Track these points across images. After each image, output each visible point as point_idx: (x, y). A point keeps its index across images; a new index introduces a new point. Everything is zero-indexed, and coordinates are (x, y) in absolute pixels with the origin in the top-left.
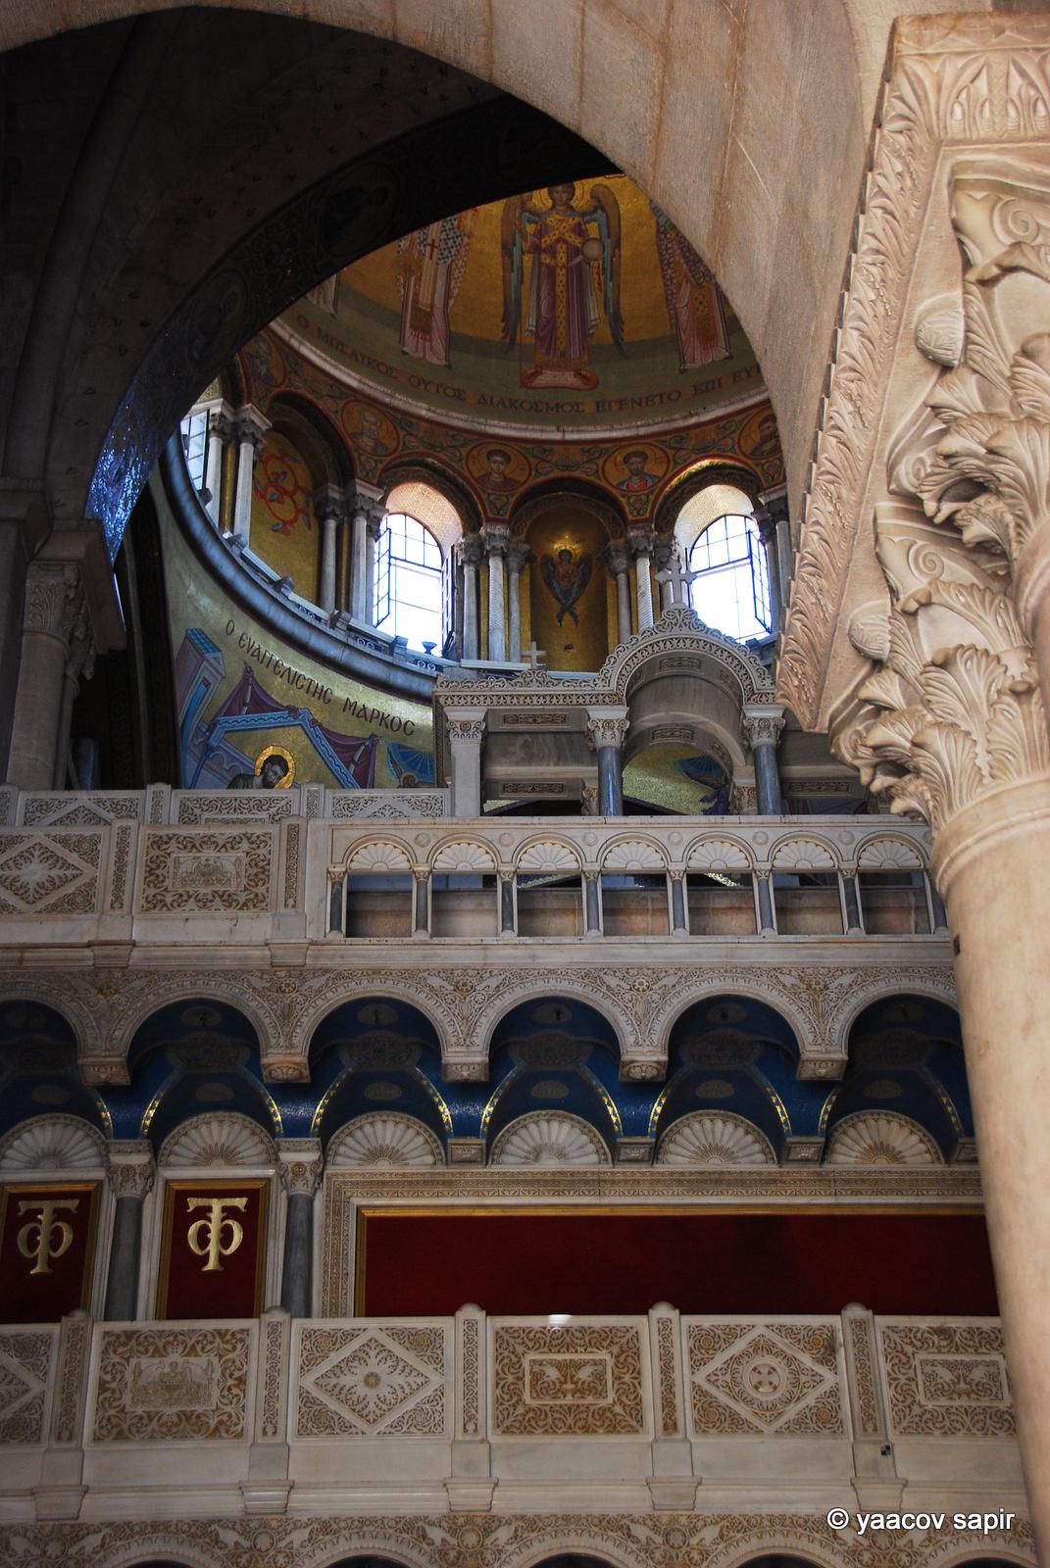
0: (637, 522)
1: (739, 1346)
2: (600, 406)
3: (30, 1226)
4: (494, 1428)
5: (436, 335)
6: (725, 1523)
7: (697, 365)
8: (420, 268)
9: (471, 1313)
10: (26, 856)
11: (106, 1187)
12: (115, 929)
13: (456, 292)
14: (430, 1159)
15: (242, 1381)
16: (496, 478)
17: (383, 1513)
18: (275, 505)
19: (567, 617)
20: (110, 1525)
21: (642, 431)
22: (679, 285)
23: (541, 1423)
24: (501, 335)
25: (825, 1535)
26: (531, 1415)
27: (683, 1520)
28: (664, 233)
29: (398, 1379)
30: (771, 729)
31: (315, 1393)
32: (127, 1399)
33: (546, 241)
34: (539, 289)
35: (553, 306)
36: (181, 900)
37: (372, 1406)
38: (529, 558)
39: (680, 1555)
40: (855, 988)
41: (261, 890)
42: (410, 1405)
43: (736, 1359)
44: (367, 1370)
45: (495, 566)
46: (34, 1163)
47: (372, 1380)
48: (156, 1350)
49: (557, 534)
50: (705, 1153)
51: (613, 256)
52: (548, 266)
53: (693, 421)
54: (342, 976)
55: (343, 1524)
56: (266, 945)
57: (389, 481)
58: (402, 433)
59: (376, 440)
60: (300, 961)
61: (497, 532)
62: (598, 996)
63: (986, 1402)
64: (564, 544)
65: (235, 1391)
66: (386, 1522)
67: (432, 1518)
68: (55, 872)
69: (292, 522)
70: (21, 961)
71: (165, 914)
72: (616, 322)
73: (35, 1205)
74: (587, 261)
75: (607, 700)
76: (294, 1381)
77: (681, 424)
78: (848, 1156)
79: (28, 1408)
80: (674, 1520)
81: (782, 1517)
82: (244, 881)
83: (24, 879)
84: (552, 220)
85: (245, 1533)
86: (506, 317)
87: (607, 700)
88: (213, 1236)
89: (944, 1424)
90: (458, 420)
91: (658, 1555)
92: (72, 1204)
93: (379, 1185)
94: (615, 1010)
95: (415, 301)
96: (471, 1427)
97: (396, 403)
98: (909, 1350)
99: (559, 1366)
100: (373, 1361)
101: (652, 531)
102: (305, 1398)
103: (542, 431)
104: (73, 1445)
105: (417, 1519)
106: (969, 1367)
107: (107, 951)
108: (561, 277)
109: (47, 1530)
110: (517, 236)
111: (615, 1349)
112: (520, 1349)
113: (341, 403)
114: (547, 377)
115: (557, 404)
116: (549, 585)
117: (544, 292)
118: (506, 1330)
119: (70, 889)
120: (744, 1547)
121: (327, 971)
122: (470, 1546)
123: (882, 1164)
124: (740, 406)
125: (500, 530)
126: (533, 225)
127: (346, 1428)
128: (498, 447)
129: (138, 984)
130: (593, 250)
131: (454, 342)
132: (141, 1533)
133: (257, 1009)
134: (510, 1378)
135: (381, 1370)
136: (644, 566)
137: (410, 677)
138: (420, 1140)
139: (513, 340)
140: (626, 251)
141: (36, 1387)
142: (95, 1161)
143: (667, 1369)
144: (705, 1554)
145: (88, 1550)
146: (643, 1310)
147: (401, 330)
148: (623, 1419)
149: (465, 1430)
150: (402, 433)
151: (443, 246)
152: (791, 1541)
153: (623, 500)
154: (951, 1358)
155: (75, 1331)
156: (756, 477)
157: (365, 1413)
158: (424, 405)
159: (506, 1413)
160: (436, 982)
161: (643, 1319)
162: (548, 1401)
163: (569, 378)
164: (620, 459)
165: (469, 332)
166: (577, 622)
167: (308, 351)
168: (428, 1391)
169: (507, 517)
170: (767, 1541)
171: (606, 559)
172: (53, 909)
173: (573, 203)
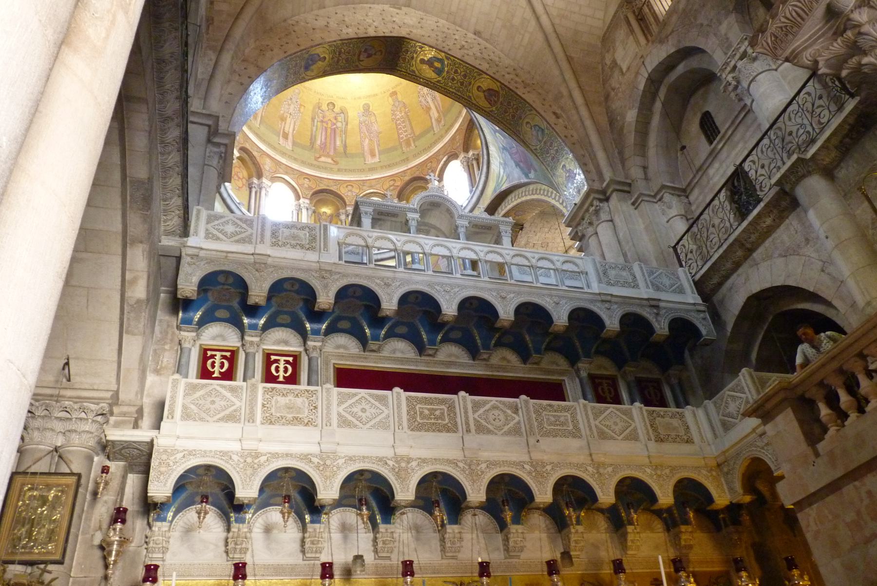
1: (487, 407)
2: (339, 170)
3: (211, 360)
5: (289, 140)
7: (370, 162)
8: (286, 119)
9: (397, 390)
10: (227, 222)
11: (241, 349)
12: (262, 249)
14: (358, 350)
15: (316, 408)
20: (270, 453)
21: (352, 179)
27: (475, 461)
29: (373, 411)
31: (344, 413)
32: (273, 411)
35: (326, 139)
36: (284, 245)
37: (364, 419)
38: (314, 212)
41: (314, 245)
42: (378, 419)
43: (488, 411)
44: (362, 407)
45: (304, 211)
46: (214, 338)
48: (283, 395)
50: (450, 355)
54: (345, 276)
56: (318, 262)
60: (330, 269)
62: (433, 292)
63: (565, 428)
65: (314, 411)
67: (389, 457)
68: (237, 229)
70: (226, 257)
71: (279, 248)
72: (345, 146)
73: (214, 353)
74: (337, 128)
76: (335, 409)
78: (495, 360)
79: (235, 411)
80: (472, 461)
82: (308, 241)
83: (226, 230)
84: (327, 113)
85: (321, 459)
86: (311, 139)
88: (281, 369)
89: (555, 434)
91: (467, 472)
92: (228, 354)
93: (341, 357)
94: (439, 297)
95: (284, 130)
98: (541, 411)
99: (429, 410)
100: (363, 404)
102: (339, 415)
104: (254, 424)
106: (559, 417)
107: (259, 257)
108: (329, 131)
109: (246, 454)
111: (447, 405)
112: (415, 403)
114: (323, 159)
117: (324, 133)
118: (410, 397)
119: (243, 235)
120: (495, 471)
121: (339, 273)
123: (505, 363)
125: (307, 201)
127: (355, 426)
129: (270, 270)
130: (339, 124)
131: (294, 144)
132: (282, 457)
133: (315, 283)
134: (412, 413)
135: (367, 407)
138: (354, 343)
139: (313, 147)
140: (349, 127)
141: (238, 404)
142: (237, 340)
143: (466, 412)
144: (482, 472)
145: (262, 462)
146: (456, 393)
148: (451, 429)
152: (510, 469)
154: (554, 414)
155: (253, 385)
160: (378, 281)
161: (455, 396)
162: (425, 421)
163: (329, 160)
164: (345, 185)
165: (299, 141)
168: (383, 415)
170: (502, 469)
172: (237, 241)
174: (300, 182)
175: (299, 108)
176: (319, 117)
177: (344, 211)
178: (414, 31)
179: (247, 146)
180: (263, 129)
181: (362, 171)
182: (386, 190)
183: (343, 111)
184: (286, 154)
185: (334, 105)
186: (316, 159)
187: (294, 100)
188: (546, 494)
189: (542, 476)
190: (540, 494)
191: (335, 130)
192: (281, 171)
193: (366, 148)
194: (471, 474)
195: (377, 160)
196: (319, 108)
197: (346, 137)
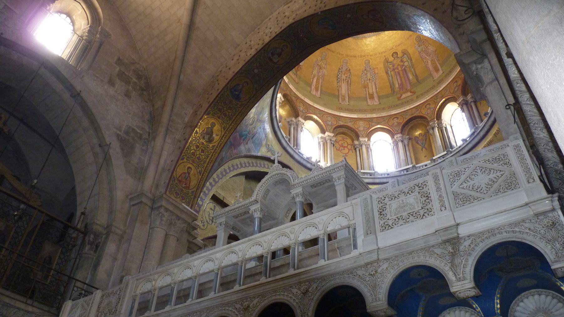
0: (431, 120)
2: (418, 97)
8: (368, 85)
13: (378, 87)
16: (396, 124)
18: (343, 151)
19: (424, 149)
21: (428, 99)
22: (428, 62)
24: (391, 91)
28: (421, 52)
30: (299, 195)
33: (396, 66)
34: (397, 77)
35: (401, 80)
38: (410, 139)
40: (258, 304)
45: (400, 144)
49: (417, 131)
51: (411, 63)
52: (398, 72)
53: (438, 91)
57: (369, 135)
58: (370, 123)
59: (364, 127)
61: (398, 136)
64: (418, 133)
69: (348, 152)
72: (416, 76)
75: (254, 203)
77: (436, 93)
84: (395, 62)
86: (391, 87)
87: (254, 203)
90: (384, 114)
97: (368, 117)
101: (435, 121)
103: (405, 108)
108: (401, 72)
110: (388, 69)
113: (353, 122)
114: (404, 96)
115: (407, 101)
116: (417, 143)
117: (398, 77)
124: (448, 83)
125: (399, 135)
126: (391, 65)
128: (395, 117)
130: (406, 64)
131: (380, 98)
136: (436, 130)
137: (380, 179)
139: (394, 91)
140: (413, 61)
147: (367, 100)
150: (370, 123)
151: (372, 78)
153: (427, 117)
156: (455, 97)
158: (375, 114)
163: (409, 94)
164: (424, 107)
166: (426, 149)
167: (342, 114)
169: (400, 132)
171: (428, 132)
173: (398, 56)
174: (390, 124)
175: (374, 71)
176: (390, 68)
177: (430, 127)
178: (298, 13)
179: (341, 123)
180: (352, 103)
181: (433, 88)
182: (454, 93)
183: (404, 53)
184: (375, 109)
185: (396, 53)
186: (399, 99)
187: (368, 69)
191: (405, 69)
192: (374, 124)
193: (431, 68)
195: (441, 72)
196: (388, 62)
197: (414, 69)
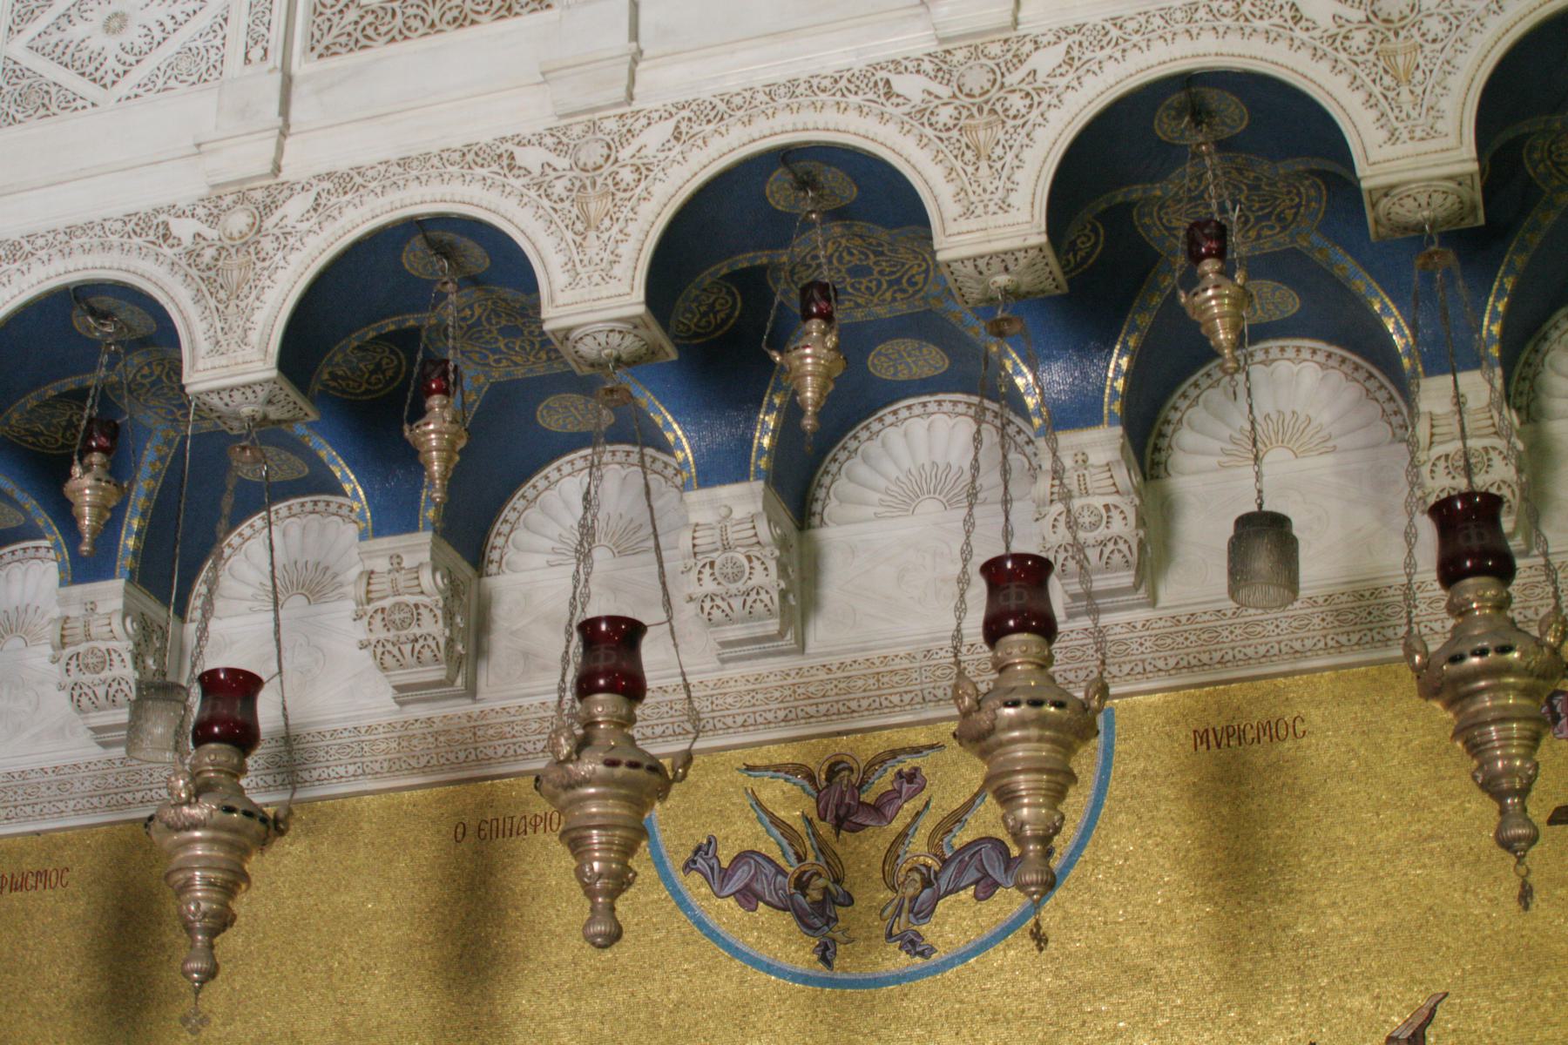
4: (304, 53)
6: (686, 113)
17: (106, 213)
23: (383, 29)
25: (871, 96)
26: (370, 18)
37: (111, 63)
39: (600, 181)
47: (115, 24)
55: (41, 242)
66: (107, 225)
67: (182, 205)
81: (794, 83)
91: (559, 188)
96: (256, 53)
105: (157, 211)
122: (236, 235)
127: (70, 103)
149: (247, 60)
157: (98, 75)
159: (325, 27)
170: (761, 126)
188: (1005, 206)
189: (997, 114)
190: (968, 213)
194: (578, 190)
